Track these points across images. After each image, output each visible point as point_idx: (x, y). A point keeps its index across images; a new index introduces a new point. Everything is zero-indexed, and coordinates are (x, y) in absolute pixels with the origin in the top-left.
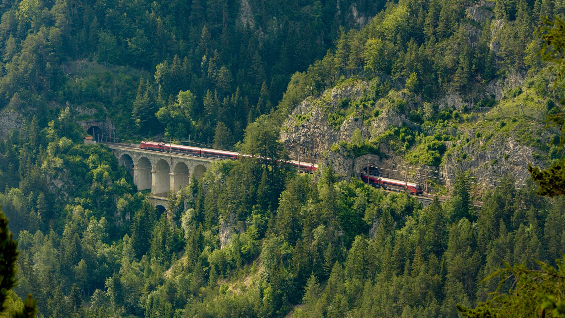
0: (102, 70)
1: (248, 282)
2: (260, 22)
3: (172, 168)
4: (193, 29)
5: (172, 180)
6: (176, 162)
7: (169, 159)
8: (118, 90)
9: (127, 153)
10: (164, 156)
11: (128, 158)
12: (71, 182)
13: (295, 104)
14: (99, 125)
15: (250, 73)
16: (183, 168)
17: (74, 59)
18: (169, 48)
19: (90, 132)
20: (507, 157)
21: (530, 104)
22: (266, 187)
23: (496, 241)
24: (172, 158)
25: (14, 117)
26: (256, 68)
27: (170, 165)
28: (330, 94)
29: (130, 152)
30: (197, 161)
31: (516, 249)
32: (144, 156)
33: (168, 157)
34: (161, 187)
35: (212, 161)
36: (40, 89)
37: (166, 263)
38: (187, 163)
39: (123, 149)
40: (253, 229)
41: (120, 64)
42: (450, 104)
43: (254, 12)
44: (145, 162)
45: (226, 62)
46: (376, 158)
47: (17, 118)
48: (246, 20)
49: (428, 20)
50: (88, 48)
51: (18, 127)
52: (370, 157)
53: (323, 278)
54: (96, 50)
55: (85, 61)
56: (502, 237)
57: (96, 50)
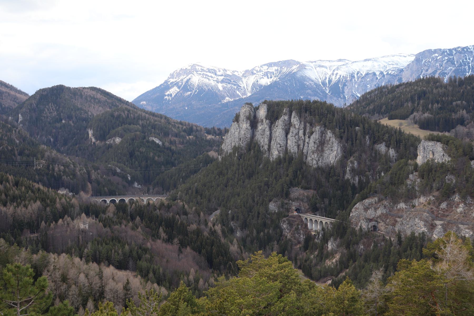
1: (334, 261)
2: (353, 177)
3: (319, 223)
4: (331, 180)
6: (320, 221)
11: (306, 219)
13: (356, 204)
16: (321, 222)
19: (296, 211)
20: (415, 225)
21: (425, 207)
22: (342, 231)
23: (405, 253)
25: (273, 204)
28: (367, 201)
31: (412, 256)
34: (314, 228)
37: (311, 253)
39: (304, 216)
42: (401, 206)
43: (350, 173)
44: (311, 220)
45: (340, 190)
46: (376, 223)
48: (348, 176)
49: (396, 179)
50: (297, 185)
52: (374, 222)
53: (355, 261)
55: (297, 188)
56: (408, 252)
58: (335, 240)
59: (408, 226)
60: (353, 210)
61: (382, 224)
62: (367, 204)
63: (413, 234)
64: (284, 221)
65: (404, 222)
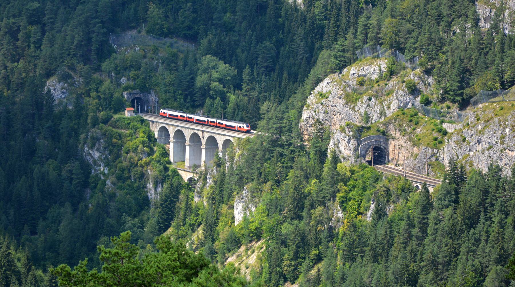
0: (152, 42)
5: (203, 152)
6: (206, 135)
7: (201, 132)
8: (163, 63)
9: (164, 125)
10: (196, 130)
11: (164, 131)
12: (107, 152)
13: (319, 81)
14: (142, 96)
15: (293, 46)
17: (123, 30)
18: (214, 22)
24: (203, 131)
26: (298, 42)
27: (202, 138)
28: (352, 71)
29: (167, 124)
30: (225, 135)
32: (179, 128)
33: (200, 130)
35: (233, 136)
36: (86, 60)
38: (216, 137)
40: (261, 206)
41: (166, 36)
44: (179, 134)
47: (62, 88)
50: (137, 21)
51: (63, 97)
54: (145, 21)
55: (134, 33)
57: (145, 21)
58: (256, 193)
59: (479, 147)
60: (311, 100)
61: (402, 141)
62: (353, 82)
63: (495, 171)
64: (95, 140)
65: (468, 134)
